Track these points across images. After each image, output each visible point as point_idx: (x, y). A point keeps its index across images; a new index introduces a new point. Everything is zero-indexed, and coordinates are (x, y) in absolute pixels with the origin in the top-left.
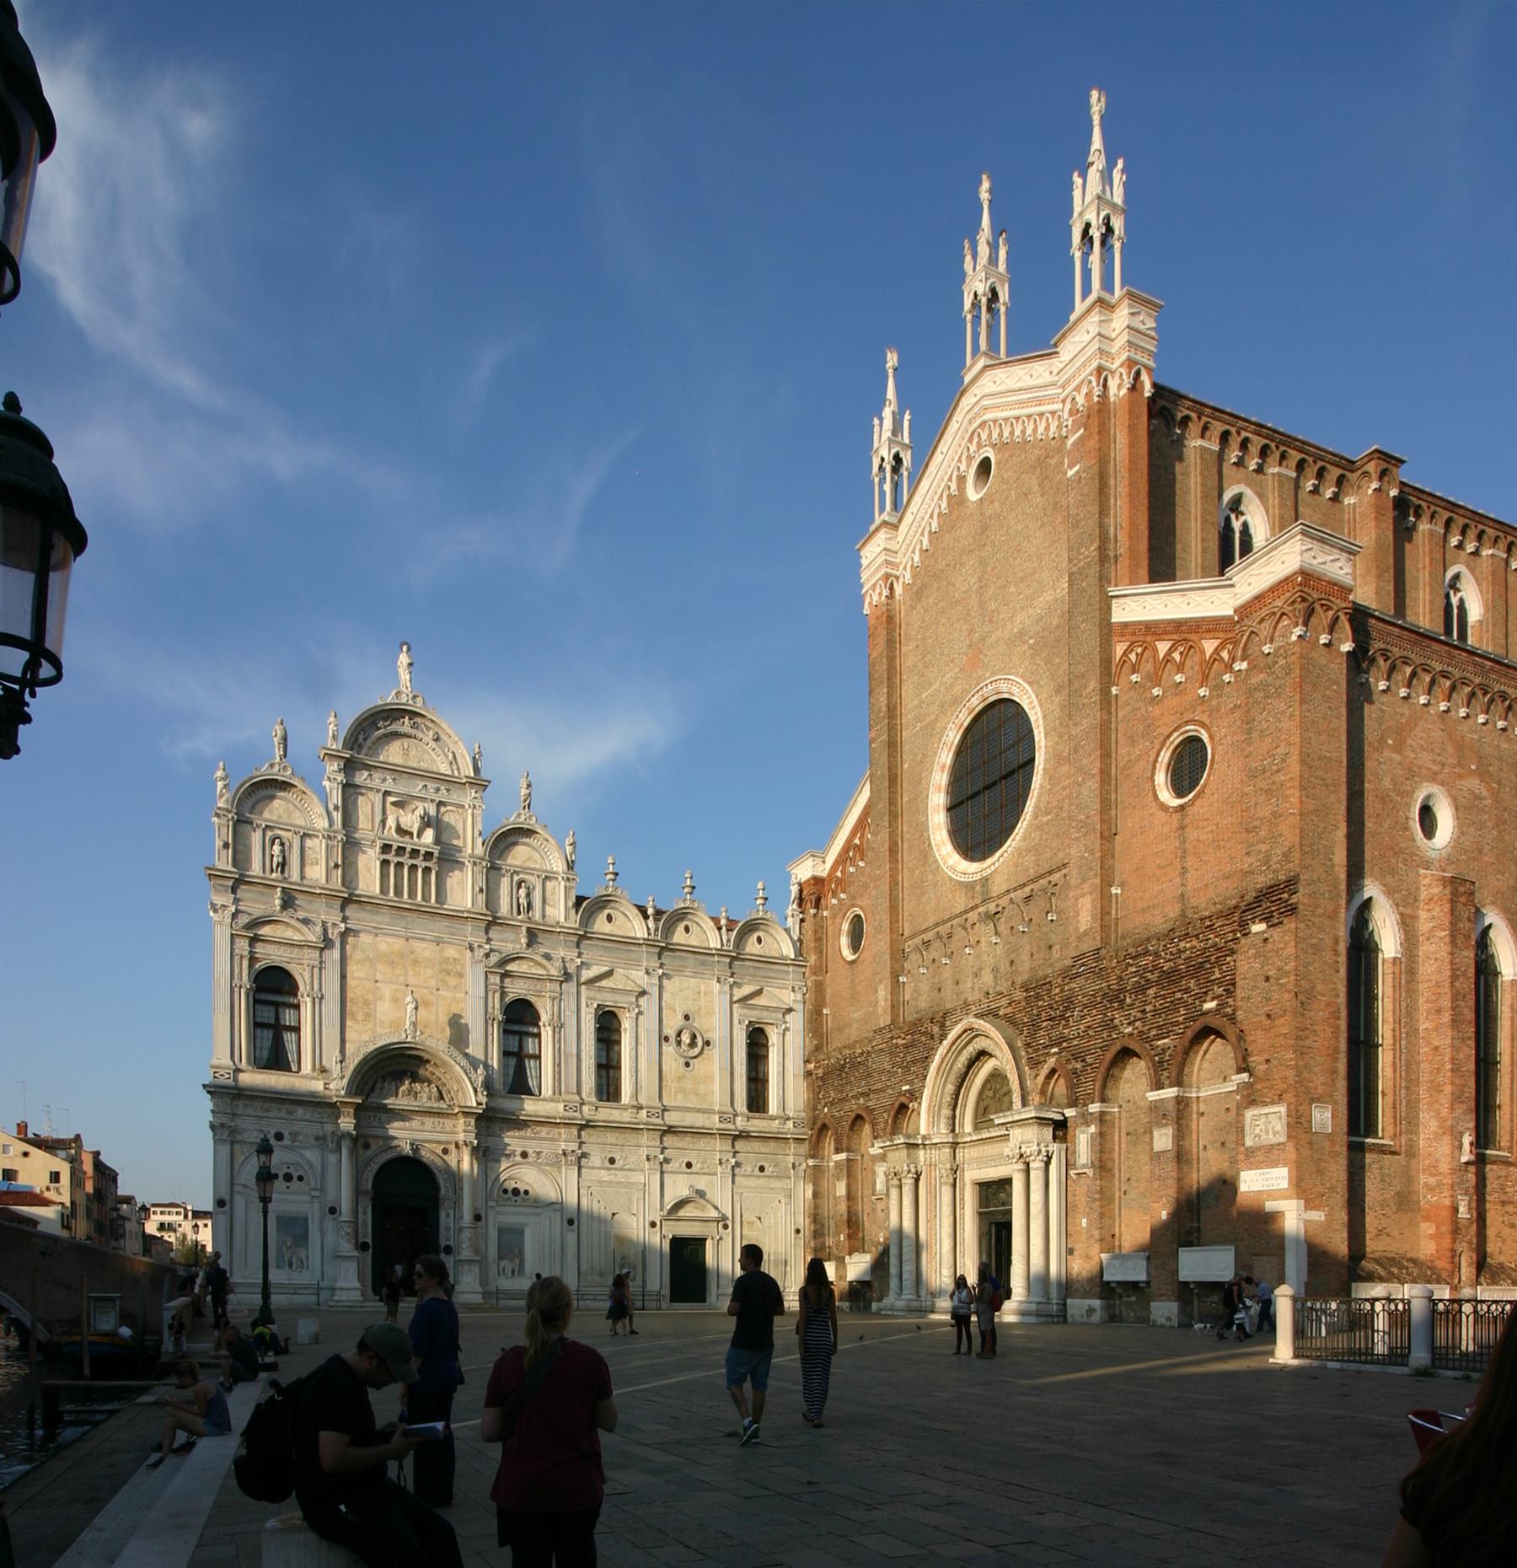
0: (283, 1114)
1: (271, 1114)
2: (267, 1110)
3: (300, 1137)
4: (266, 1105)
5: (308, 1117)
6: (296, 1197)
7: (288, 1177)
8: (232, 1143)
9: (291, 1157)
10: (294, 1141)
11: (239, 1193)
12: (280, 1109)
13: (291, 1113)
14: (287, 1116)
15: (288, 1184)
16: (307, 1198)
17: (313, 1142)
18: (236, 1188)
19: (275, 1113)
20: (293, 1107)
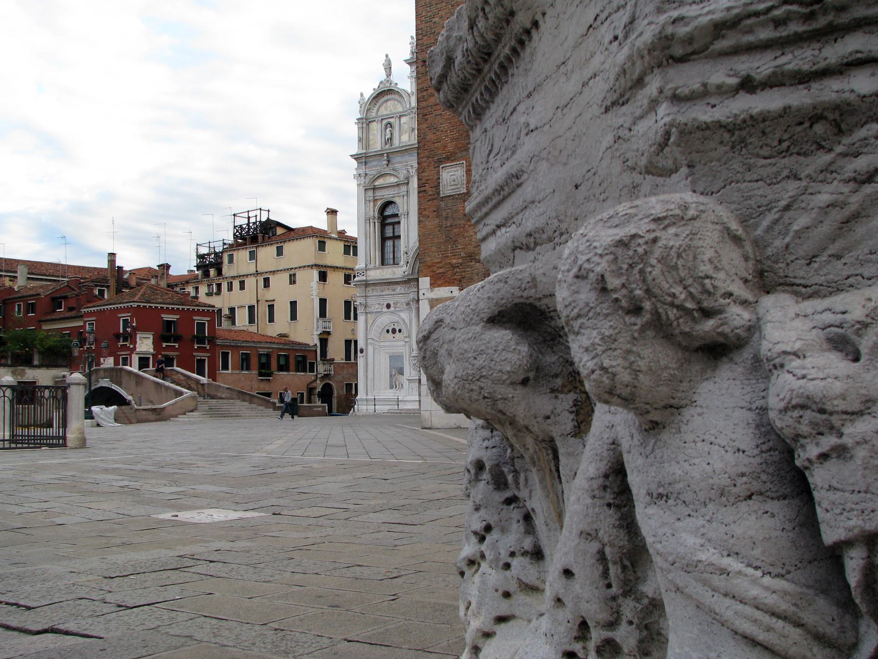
0: (390, 292)
1: (384, 293)
2: (382, 291)
3: (399, 305)
4: (382, 288)
5: (402, 291)
6: (396, 343)
7: (394, 331)
8: (366, 313)
9: (395, 318)
10: (395, 308)
11: (370, 343)
12: (388, 289)
13: (394, 290)
14: (393, 293)
15: (394, 335)
16: (403, 343)
17: (405, 307)
18: (369, 341)
19: (386, 292)
20: (395, 286)
